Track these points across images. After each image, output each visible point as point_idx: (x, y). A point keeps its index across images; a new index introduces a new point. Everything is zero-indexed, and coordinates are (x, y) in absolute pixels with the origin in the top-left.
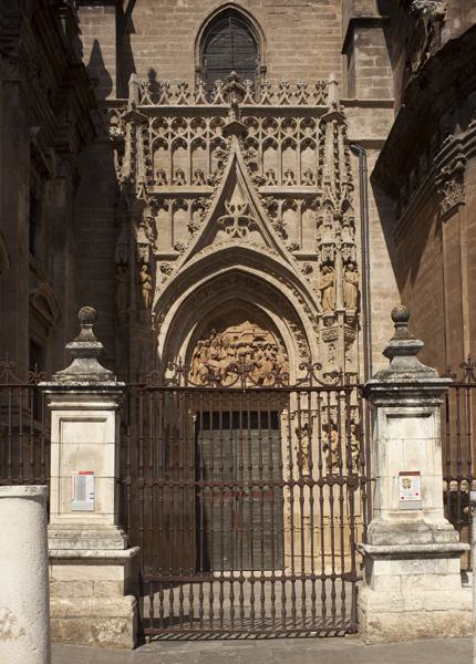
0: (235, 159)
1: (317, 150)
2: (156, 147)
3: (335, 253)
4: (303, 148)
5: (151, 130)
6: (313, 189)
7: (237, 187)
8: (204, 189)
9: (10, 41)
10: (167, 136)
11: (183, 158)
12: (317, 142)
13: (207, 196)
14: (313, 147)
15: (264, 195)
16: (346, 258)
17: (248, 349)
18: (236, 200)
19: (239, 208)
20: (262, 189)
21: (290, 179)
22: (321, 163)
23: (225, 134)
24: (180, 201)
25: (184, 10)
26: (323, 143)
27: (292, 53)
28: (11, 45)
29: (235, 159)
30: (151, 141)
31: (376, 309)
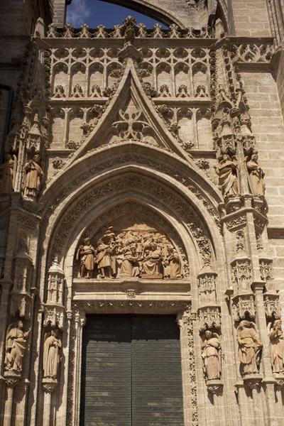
0: (130, 75)
1: (209, 73)
2: (57, 70)
3: (236, 144)
4: (195, 71)
5: (53, 57)
6: (208, 99)
7: (131, 102)
8: (99, 98)
11: (80, 78)
12: (208, 65)
13: (103, 103)
14: (204, 71)
15: (157, 103)
16: (247, 149)
18: (131, 109)
20: (154, 99)
21: (183, 92)
23: (121, 60)
24: (77, 108)
26: (213, 64)
29: (130, 75)
30: (53, 65)
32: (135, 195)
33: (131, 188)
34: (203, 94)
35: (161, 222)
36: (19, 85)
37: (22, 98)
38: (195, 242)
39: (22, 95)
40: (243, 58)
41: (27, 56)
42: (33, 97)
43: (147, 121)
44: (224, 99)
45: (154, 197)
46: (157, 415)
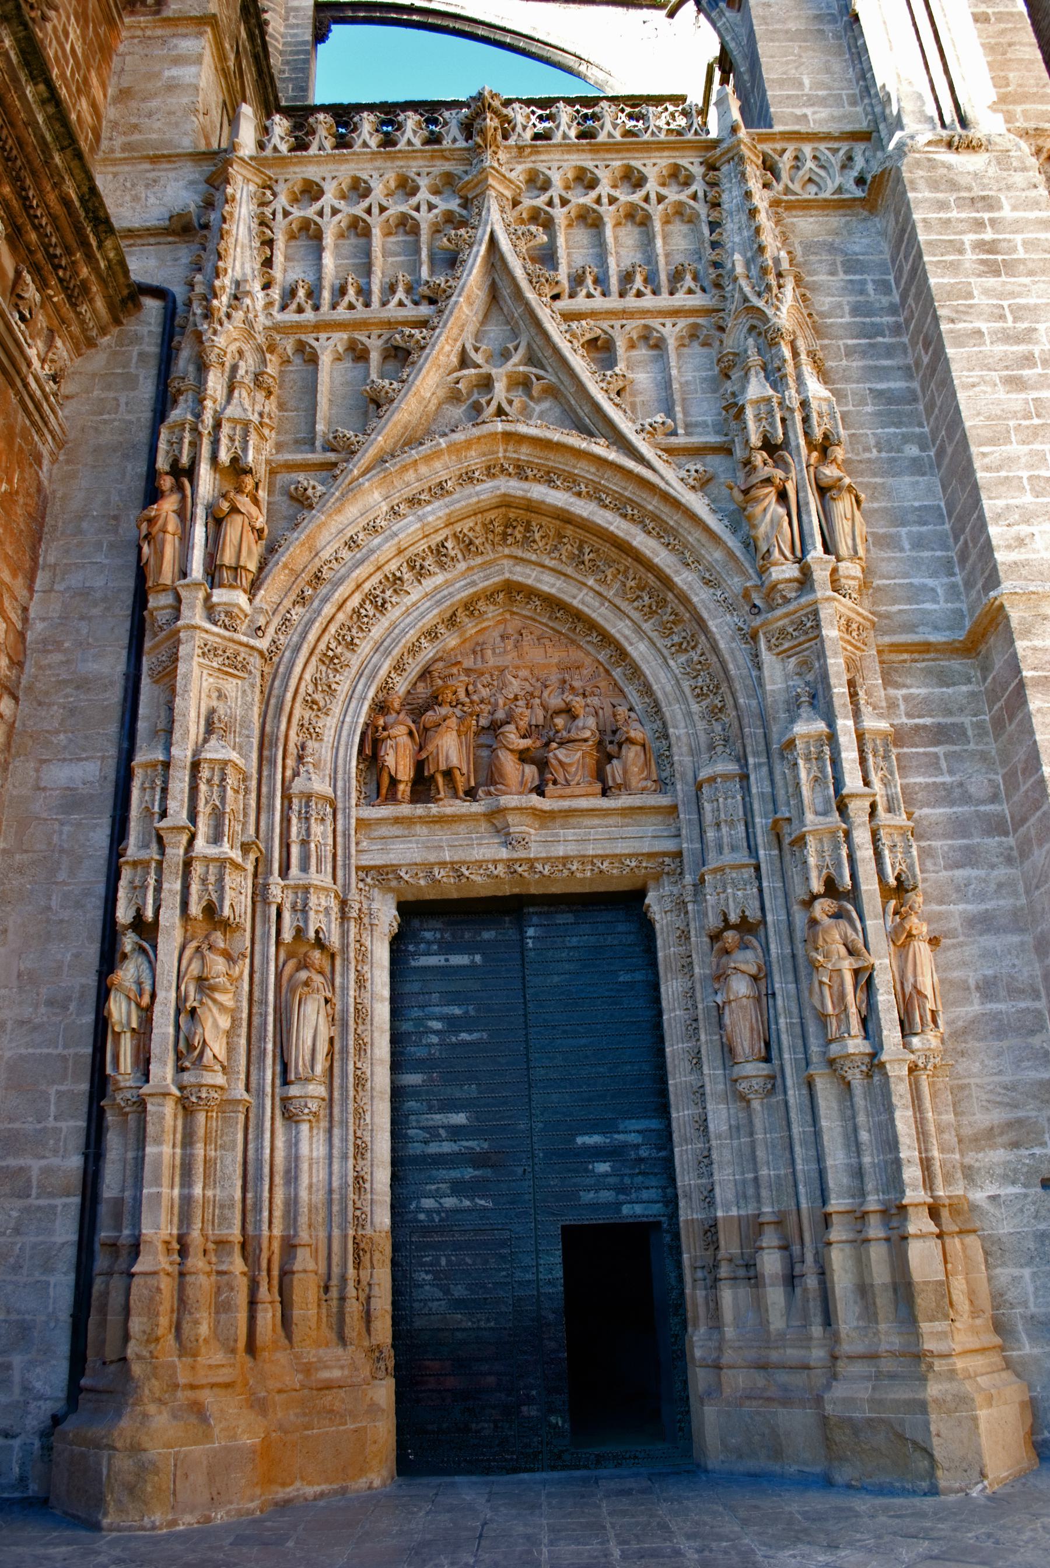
15: (568, 317)
32: (518, 569)
33: (507, 551)
34: (692, 285)
35: (594, 638)
36: (191, 286)
37: (198, 319)
38: (687, 691)
39: (199, 311)
40: (796, 187)
41: (209, 204)
42: (229, 316)
43: (543, 368)
44: (746, 300)
45: (569, 571)
46: (603, 1167)
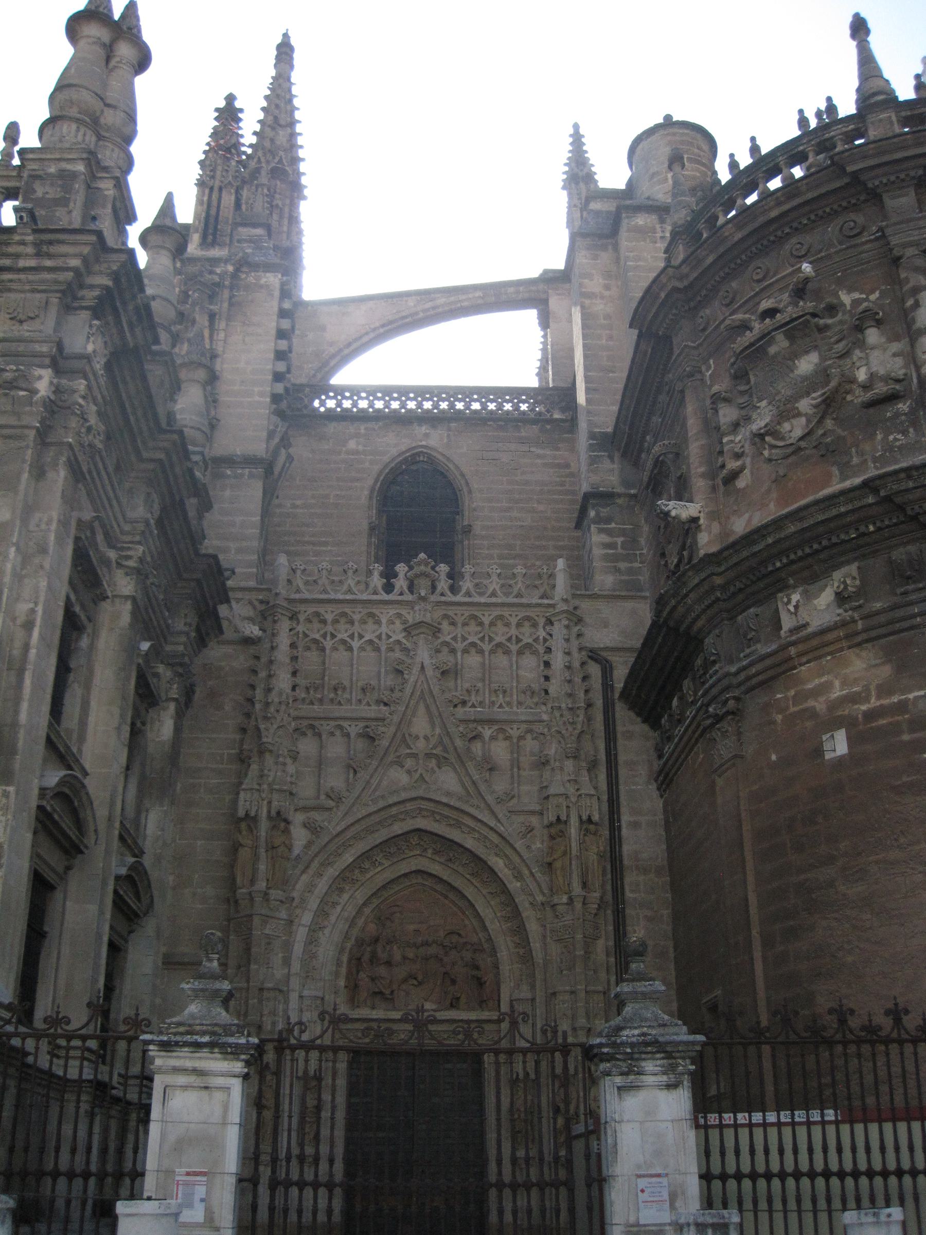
3: (568, 807)
9: (129, 549)
10: (324, 636)
16: (584, 818)
17: (433, 950)
19: (426, 738)
22: (547, 678)
25: (357, 452)
27: (508, 509)
28: (129, 553)
31: (632, 891)
